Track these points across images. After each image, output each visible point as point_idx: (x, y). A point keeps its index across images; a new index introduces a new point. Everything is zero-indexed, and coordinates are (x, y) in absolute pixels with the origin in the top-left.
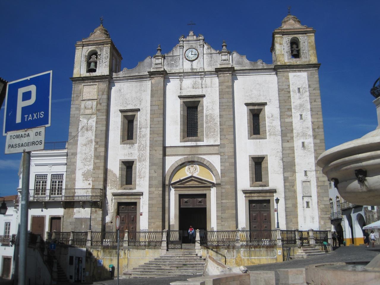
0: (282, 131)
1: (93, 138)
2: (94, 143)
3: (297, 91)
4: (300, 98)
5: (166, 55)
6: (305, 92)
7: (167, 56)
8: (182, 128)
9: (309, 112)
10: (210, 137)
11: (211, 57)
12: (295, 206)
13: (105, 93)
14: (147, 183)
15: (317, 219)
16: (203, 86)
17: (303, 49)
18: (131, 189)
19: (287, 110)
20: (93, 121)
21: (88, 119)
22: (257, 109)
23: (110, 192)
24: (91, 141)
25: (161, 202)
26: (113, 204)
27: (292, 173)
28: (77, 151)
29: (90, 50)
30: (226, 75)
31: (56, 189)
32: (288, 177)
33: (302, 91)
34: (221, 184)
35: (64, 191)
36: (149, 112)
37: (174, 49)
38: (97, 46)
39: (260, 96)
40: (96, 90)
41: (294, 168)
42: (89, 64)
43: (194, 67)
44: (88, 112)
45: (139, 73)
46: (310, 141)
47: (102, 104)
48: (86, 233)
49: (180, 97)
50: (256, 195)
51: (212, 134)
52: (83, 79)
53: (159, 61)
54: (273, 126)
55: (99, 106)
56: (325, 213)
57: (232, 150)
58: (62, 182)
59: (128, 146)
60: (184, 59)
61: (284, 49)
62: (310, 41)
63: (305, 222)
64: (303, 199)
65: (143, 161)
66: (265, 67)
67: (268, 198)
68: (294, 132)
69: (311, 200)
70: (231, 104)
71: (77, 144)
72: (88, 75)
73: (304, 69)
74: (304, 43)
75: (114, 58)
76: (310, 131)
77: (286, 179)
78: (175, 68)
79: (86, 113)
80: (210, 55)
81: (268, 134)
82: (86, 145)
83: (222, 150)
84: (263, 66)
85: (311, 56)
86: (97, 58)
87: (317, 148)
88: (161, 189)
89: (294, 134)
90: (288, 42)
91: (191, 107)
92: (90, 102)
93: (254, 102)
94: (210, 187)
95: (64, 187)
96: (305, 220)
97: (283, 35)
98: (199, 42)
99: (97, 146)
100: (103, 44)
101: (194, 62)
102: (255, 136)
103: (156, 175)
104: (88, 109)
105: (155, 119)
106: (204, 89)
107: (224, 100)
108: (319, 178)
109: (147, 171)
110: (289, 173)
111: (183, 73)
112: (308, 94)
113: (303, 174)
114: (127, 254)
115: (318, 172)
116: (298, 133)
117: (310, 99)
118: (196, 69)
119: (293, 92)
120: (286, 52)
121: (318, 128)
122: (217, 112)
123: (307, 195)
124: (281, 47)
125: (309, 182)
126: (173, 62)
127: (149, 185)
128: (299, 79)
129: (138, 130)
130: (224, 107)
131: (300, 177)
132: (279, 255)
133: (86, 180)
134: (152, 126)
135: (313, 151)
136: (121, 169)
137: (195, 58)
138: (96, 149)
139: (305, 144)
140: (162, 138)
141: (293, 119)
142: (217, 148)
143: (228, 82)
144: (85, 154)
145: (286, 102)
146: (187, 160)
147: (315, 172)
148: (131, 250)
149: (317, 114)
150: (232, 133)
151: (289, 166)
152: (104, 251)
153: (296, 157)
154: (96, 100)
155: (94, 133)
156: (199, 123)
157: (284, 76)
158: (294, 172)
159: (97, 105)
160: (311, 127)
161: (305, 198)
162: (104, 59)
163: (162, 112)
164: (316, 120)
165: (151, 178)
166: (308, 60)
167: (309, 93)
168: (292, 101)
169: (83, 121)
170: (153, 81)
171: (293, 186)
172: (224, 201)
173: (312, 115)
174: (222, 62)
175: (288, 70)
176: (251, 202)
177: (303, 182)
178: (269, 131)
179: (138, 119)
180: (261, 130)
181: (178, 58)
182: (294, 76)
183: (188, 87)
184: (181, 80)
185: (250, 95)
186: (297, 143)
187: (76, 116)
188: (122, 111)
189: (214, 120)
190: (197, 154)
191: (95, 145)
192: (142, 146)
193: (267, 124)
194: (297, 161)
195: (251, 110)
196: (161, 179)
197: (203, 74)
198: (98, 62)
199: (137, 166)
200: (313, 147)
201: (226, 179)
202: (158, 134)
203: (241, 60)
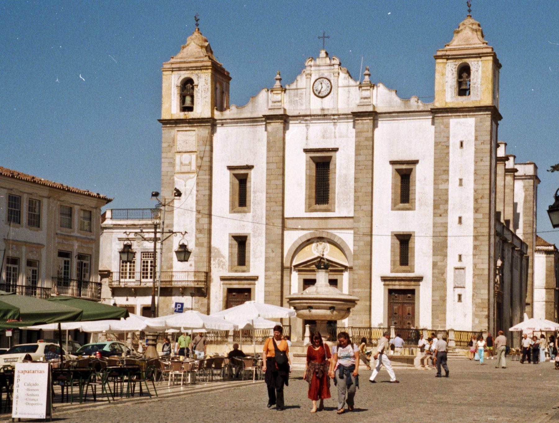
3: (459, 145)
5: (287, 87)
7: (289, 89)
8: (308, 194)
11: (349, 92)
12: (443, 299)
13: (208, 143)
16: (337, 135)
17: (475, 81)
18: (243, 271)
22: (406, 169)
23: (216, 275)
25: (280, 289)
27: (442, 257)
29: (183, 77)
30: (364, 121)
32: (437, 262)
34: (354, 268)
37: (299, 78)
38: (193, 72)
40: (194, 138)
41: (445, 251)
43: (326, 107)
44: (185, 169)
46: (469, 217)
49: (306, 151)
50: (397, 283)
52: (176, 122)
53: (278, 97)
55: (199, 160)
65: (259, 236)
66: (421, 109)
67: (411, 288)
72: (182, 115)
73: (471, 114)
77: (435, 265)
79: (183, 171)
80: (347, 88)
83: (356, 225)
84: (418, 106)
86: (193, 88)
87: (478, 225)
88: (279, 273)
90: (454, 70)
91: (322, 165)
94: (342, 271)
97: (448, 59)
98: (332, 67)
99: (200, 216)
100: (200, 68)
101: (324, 99)
104: (186, 165)
108: (478, 265)
111: (310, 116)
112: (473, 149)
115: (477, 257)
117: (476, 157)
118: (328, 109)
120: (449, 86)
122: (353, 171)
123: (459, 286)
125: (463, 269)
126: (297, 99)
127: (266, 267)
128: (463, 128)
129: (252, 195)
130: (360, 168)
131: (452, 262)
136: (231, 246)
137: (327, 93)
138: (198, 220)
142: (351, 220)
143: (368, 132)
146: (313, 237)
149: (483, 178)
151: (440, 247)
154: (196, 153)
157: (443, 123)
158: (446, 256)
161: (456, 289)
162: (203, 93)
163: (281, 172)
165: (267, 260)
166: (479, 99)
167: (475, 148)
172: (356, 290)
173: (475, 180)
174: (363, 100)
175: (450, 114)
177: (456, 269)
178: (420, 200)
181: (304, 93)
186: (452, 219)
187: (169, 174)
188: (230, 168)
190: (327, 229)
191: (196, 215)
194: (450, 241)
196: (280, 260)
202: (276, 202)
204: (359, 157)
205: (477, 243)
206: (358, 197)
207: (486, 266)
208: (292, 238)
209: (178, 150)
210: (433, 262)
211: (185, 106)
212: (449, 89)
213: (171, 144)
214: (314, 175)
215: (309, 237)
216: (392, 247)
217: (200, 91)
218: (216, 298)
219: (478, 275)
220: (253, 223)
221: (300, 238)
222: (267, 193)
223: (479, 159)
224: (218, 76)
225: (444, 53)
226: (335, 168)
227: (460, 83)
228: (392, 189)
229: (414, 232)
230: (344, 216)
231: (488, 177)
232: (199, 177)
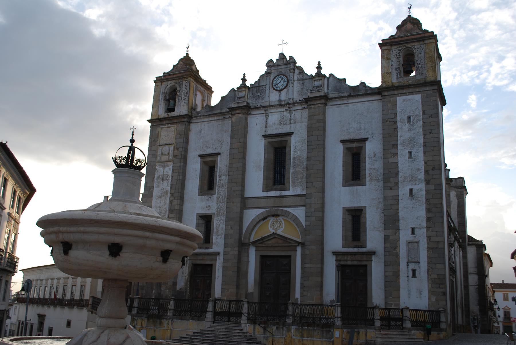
0: (384, 174)
1: (169, 189)
2: (169, 195)
3: (406, 121)
4: (410, 130)
6: (417, 122)
9: (422, 149)
11: (303, 84)
12: (397, 275)
15: (426, 293)
16: (292, 121)
18: (207, 248)
21: (164, 167)
22: (356, 147)
33: (414, 120)
39: (360, 129)
40: (173, 133)
41: (397, 224)
42: (168, 101)
43: (283, 98)
44: (164, 158)
46: (420, 188)
48: (238, 302)
49: (265, 136)
50: (349, 258)
51: (300, 181)
54: (375, 169)
55: (176, 151)
59: (206, 197)
60: (271, 89)
61: (392, 65)
62: (428, 50)
63: (409, 297)
64: (408, 266)
65: (222, 215)
67: (364, 263)
68: (399, 176)
69: (419, 267)
72: (166, 115)
74: (421, 53)
75: (198, 93)
76: (422, 174)
77: (386, 239)
78: (260, 101)
80: (301, 82)
81: (368, 179)
82: (161, 197)
88: (236, 249)
89: (400, 179)
91: (278, 148)
92: (167, 147)
93: (352, 138)
97: (391, 46)
98: (289, 66)
104: (165, 155)
106: (293, 125)
112: (421, 123)
113: (410, 232)
114: (170, 325)
115: (431, 229)
116: (405, 177)
118: (285, 101)
119: (401, 122)
121: (432, 169)
123: (413, 260)
124: (389, 62)
125: (417, 242)
126: (259, 94)
127: (225, 243)
129: (218, 179)
131: (404, 236)
132: (337, 338)
135: (425, 201)
138: (171, 202)
139: (414, 191)
141: (399, 158)
142: (304, 198)
144: (160, 207)
148: (175, 320)
151: (391, 221)
152: (148, 320)
158: (398, 229)
161: (410, 265)
165: (227, 236)
166: (424, 77)
168: (399, 134)
170: (234, 119)
172: (307, 266)
173: (425, 153)
175: (396, 92)
177: (409, 242)
178: (370, 176)
179: (219, 165)
183: (275, 124)
184: (267, 116)
185: (347, 129)
186: (403, 191)
188: (201, 156)
192: (221, 197)
193: (368, 166)
194: (401, 214)
198: (177, 99)
200: (424, 195)
205: (430, 215)
210: (385, 236)
215: (265, 215)
216: (343, 222)
218: (183, 273)
219: (432, 248)
224: (200, 86)
228: (343, 166)
230: (297, 194)
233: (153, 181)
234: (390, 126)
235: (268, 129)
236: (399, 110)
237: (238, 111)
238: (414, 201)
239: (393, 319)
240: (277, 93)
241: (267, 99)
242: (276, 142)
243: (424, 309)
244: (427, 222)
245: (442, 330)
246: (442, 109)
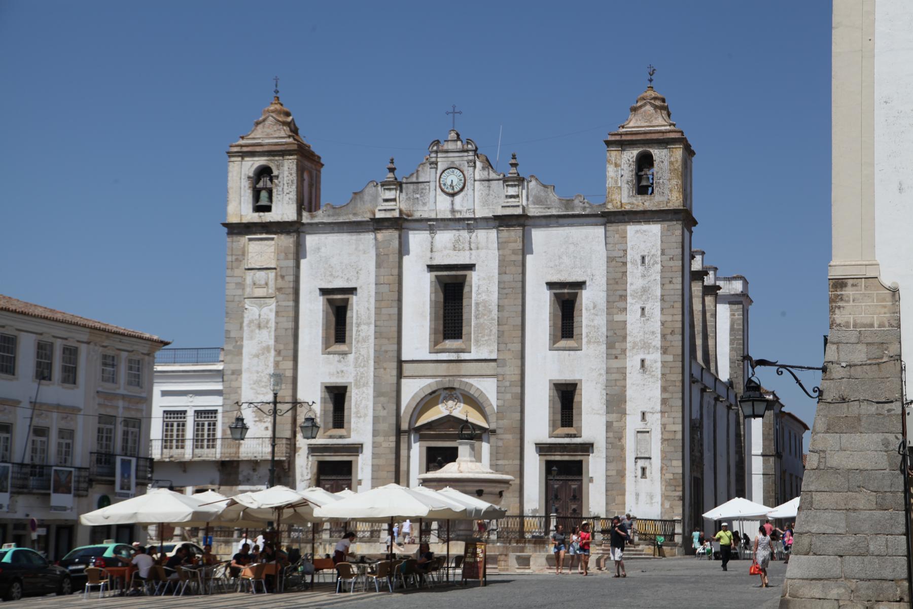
2: (273, 353)
3: (639, 262)
4: (643, 276)
6: (653, 264)
9: (659, 304)
10: (481, 344)
11: (489, 187)
12: (622, 474)
13: (291, 256)
14: (370, 428)
15: (658, 499)
16: (473, 246)
18: (341, 437)
19: (617, 299)
20: (271, 310)
21: (260, 306)
24: (268, 349)
25: (393, 462)
26: (310, 463)
28: (241, 366)
29: (257, 165)
31: (205, 437)
32: (612, 422)
34: (498, 431)
35: (219, 443)
36: (373, 293)
40: (272, 249)
45: (355, 214)
46: (655, 358)
47: (287, 278)
49: (431, 268)
51: (486, 338)
54: (594, 327)
55: (280, 280)
56: (673, 488)
57: (518, 371)
58: (214, 425)
59: (336, 357)
60: (439, 190)
62: (672, 159)
65: (364, 386)
67: (578, 458)
69: (651, 464)
70: (520, 284)
71: (241, 354)
72: (256, 217)
77: (609, 425)
78: (420, 208)
80: (486, 183)
81: (584, 340)
82: (257, 356)
83: (500, 371)
85: (671, 191)
86: (271, 180)
88: (393, 439)
91: (451, 288)
92: (263, 273)
95: (219, 434)
96: (637, 499)
98: (466, 154)
99: (280, 358)
100: (283, 153)
102: (563, 343)
103: (383, 413)
104: (260, 287)
105: (384, 311)
106: (473, 252)
107: (507, 278)
109: (371, 405)
110: (615, 415)
112: (658, 267)
116: (634, 343)
117: (662, 278)
118: (460, 212)
122: (495, 296)
123: (643, 456)
126: (418, 196)
127: (374, 431)
128: (645, 238)
129: (354, 329)
130: (505, 291)
131: (632, 423)
133: (260, 421)
134: (378, 323)
135: (660, 376)
136: (324, 401)
138: (277, 364)
139: (647, 363)
140: (395, 347)
142: (493, 364)
143: (516, 242)
144: (258, 372)
145: (617, 283)
146: (441, 386)
147: (659, 415)
150: (519, 339)
151: (616, 402)
153: (628, 386)
155: (273, 333)
156: (465, 317)
157: (617, 232)
158: (624, 413)
159: (276, 279)
160: (659, 331)
161: (639, 461)
162: (286, 187)
163: (396, 297)
164: (669, 318)
165: (376, 419)
166: (664, 199)
168: (629, 280)
169: (252, 311)
171: (620, 439)
172: (500, 462)
173: (662, 309)
176: (549, 465)
177: (638, 432)
178: (587, 336)
179: (355, 307)
180: (576, 331)
182: (637, 232)
186: (632, 362)
187: (237, 299)
188: (324, 292)
189: (490, 312)
191: (275, 357)
193: (585, 322)
194: (629, 393)
195: (555, 294)
196: (393, 420)
197: (470, 224)
198: (274, 191)
199: (353, 395)
201: (505, 423)
202: (389, 339)
203: (543, 194)
204: (504, 276)
205: (666, 395)
206: (503, 332)
207: (679, 428)
208: (412, 389)
209: (250, 266)
211: (259, 204)
212: (626, 186)
213: (240, 258)
214: (442, 300)
215: (434, 389)
217: (281, 184)
218: (302, 476)
220: (356, 368)
221: (422, 389)
222: (376, 326)
223: (667, 281)
225: (618, 138)
226: (471, 291)
227: (639, 178)
229: (581, 380)
230: (483, 357)
231: (679, 305)
232: (280, 303)
233: (241, 328)
234: (617, 266)
235: (435, 255)
236: (629, 244)
237: (386, 224)
238: (646, 376)
239: (619, 534)
240: (449, 198)
241: (431, 205)
242: (448, 276)
243: (656, 518)
244: (662, 404)
245: (675, 545)
246: (691, 232)
